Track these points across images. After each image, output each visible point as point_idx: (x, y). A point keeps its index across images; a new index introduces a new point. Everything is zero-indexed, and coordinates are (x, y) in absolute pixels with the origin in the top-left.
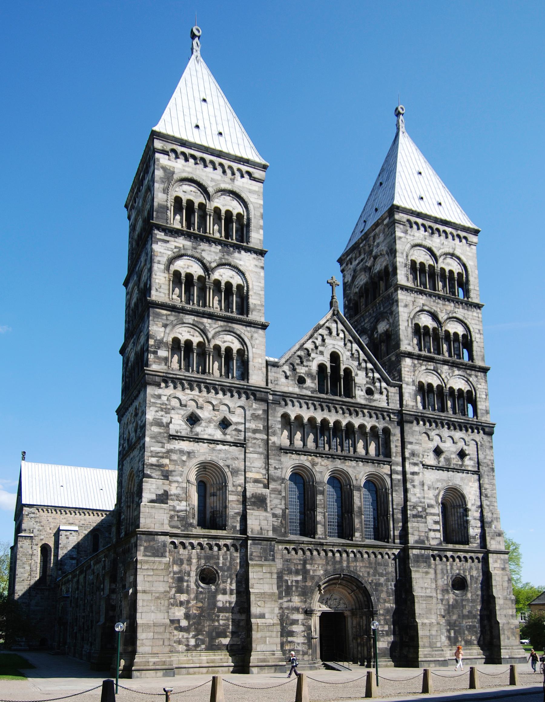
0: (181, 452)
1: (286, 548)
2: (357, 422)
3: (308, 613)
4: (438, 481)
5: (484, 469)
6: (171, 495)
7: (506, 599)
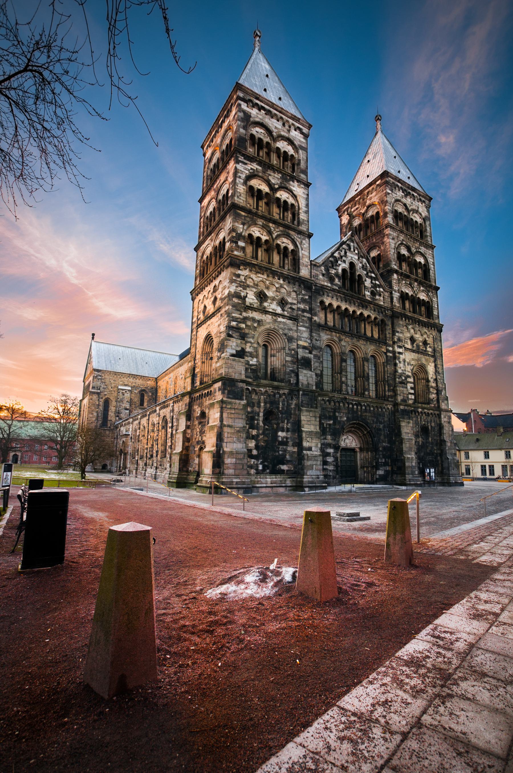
0: (253, 320)
1: (323, 399)
2: (366, 313)
3: (336, 447)
4: (413, 359)
5: (438, 355)
6: (246, 352)
7: (451, 443)
